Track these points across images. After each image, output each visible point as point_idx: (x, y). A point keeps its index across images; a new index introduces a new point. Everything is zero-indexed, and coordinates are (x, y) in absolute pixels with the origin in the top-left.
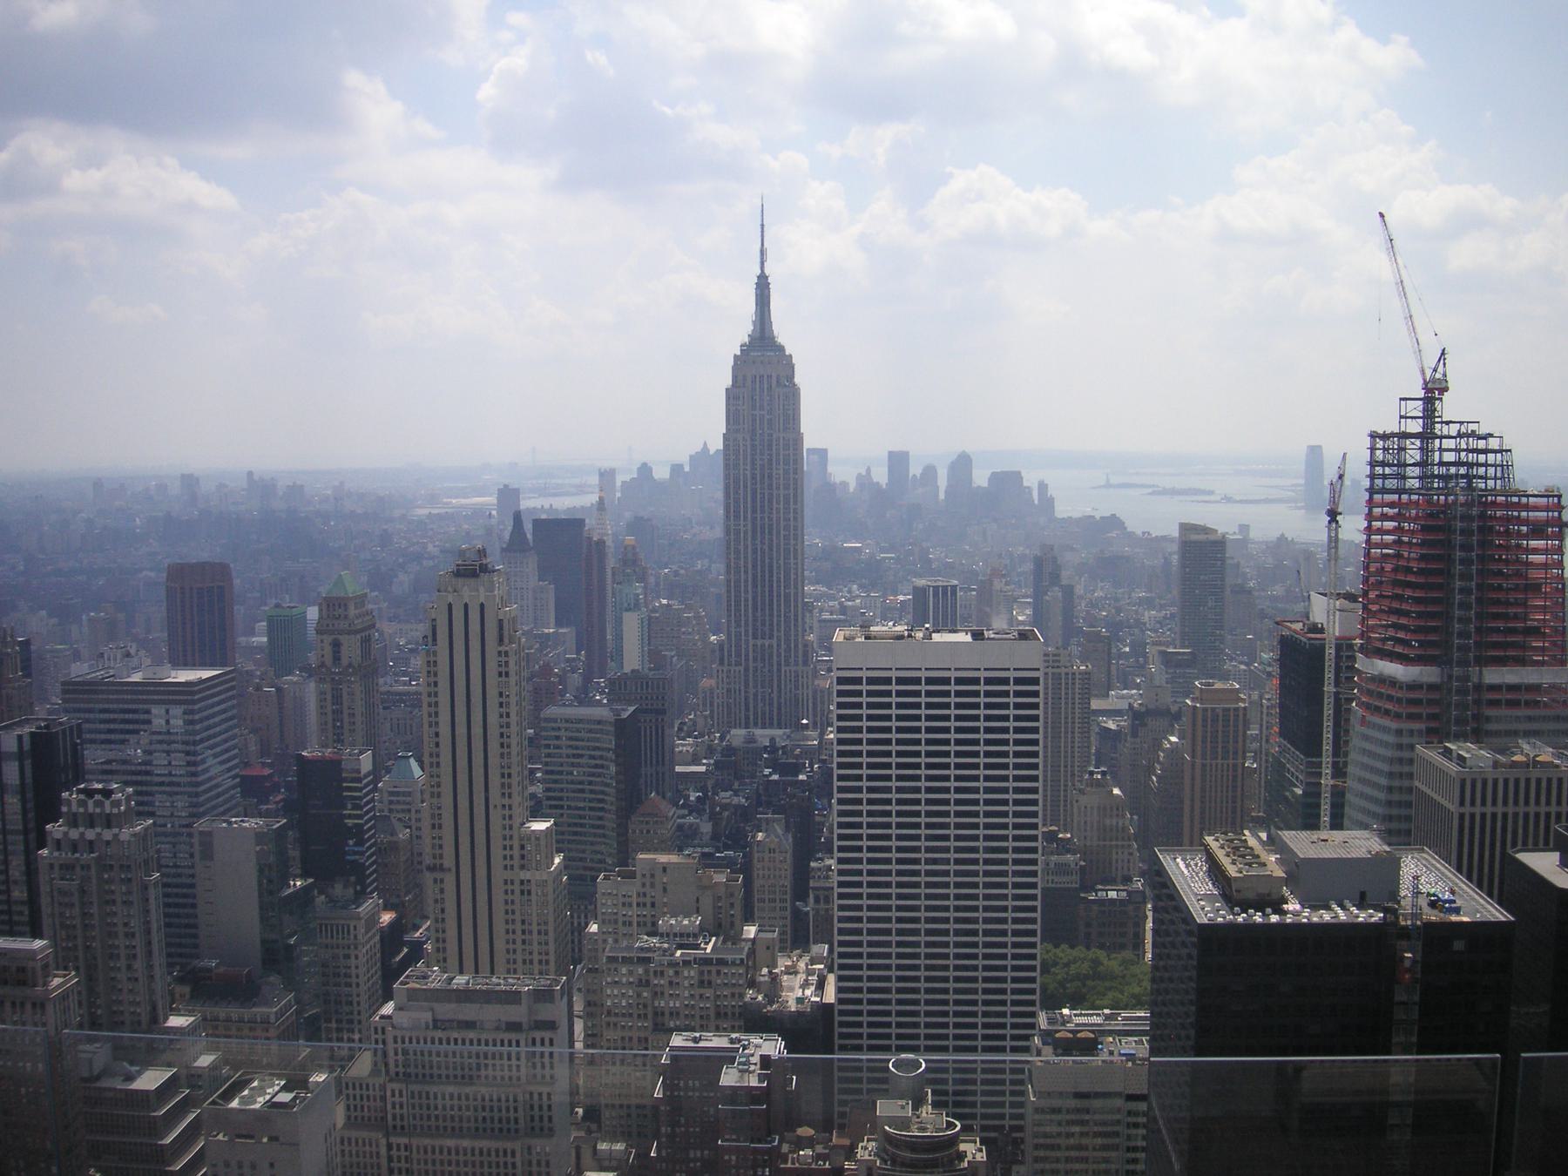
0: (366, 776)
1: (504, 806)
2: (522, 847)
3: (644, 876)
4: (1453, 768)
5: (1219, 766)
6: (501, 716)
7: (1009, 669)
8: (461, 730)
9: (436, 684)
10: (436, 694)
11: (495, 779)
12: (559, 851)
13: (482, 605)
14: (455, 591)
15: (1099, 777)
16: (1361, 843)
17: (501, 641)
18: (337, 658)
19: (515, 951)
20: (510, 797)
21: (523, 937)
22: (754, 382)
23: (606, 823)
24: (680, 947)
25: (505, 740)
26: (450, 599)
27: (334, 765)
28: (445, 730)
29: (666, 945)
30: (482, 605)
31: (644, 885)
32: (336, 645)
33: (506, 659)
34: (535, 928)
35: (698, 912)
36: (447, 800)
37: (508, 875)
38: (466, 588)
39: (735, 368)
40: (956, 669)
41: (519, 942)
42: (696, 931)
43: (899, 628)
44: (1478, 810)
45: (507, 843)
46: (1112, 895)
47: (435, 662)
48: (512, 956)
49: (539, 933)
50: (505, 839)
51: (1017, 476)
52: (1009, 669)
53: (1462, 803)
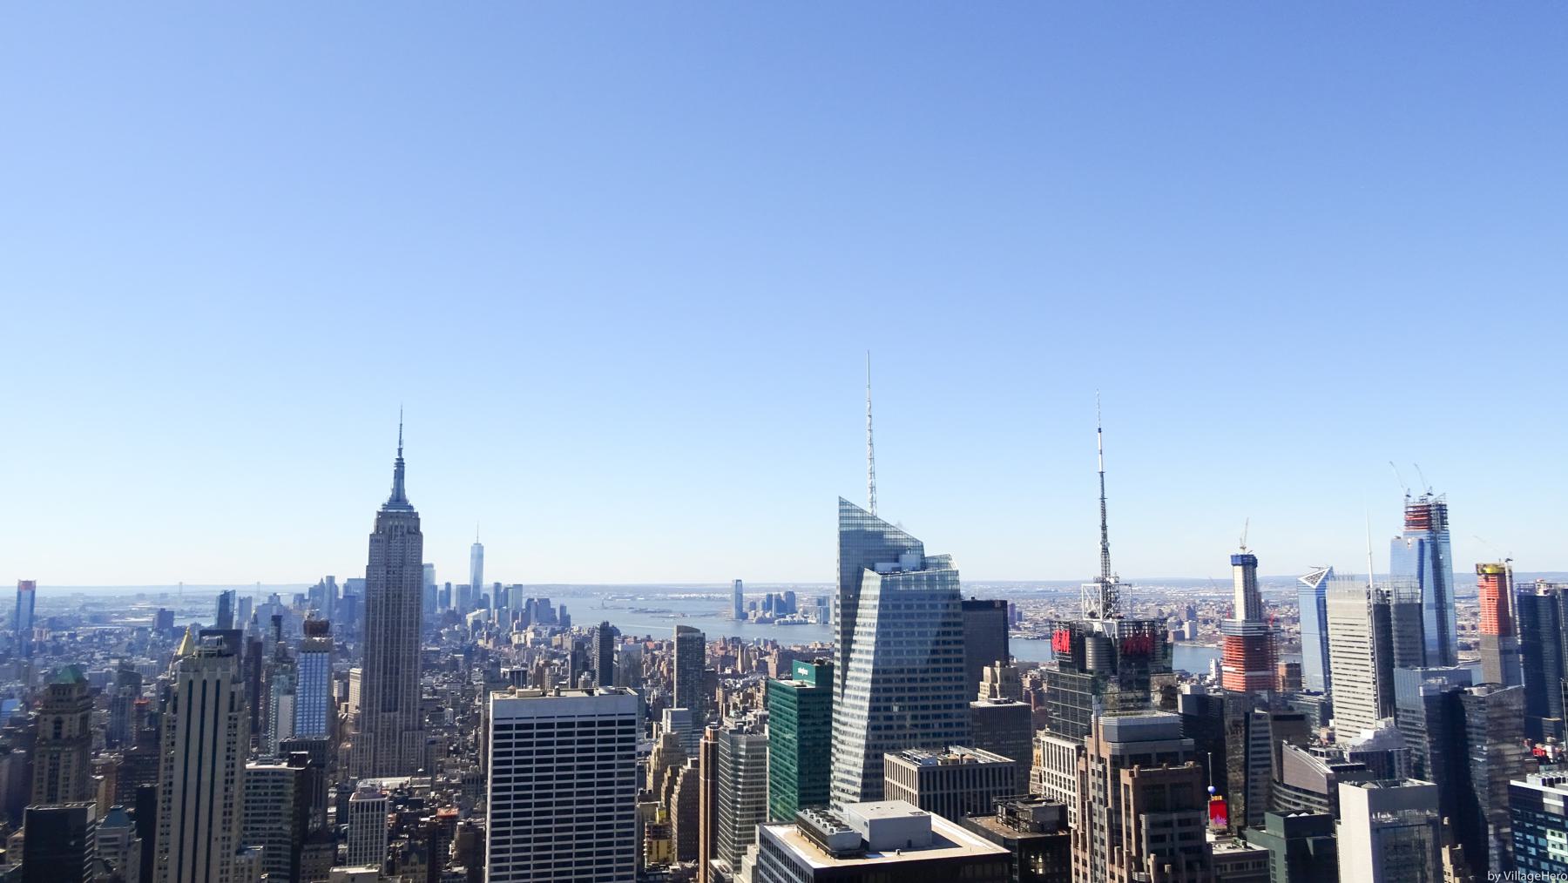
0: (94, 822)
1: (224, 838)
6: (227, 767)
7: (614, 715)
8: (192, 779)
12: (264, 871)
13: (218, 682)
14: (196, 671)
16: (900, 808)
17: (232, 709)
18: (57, 735)
20: (230, 830)
23: (283, 853)
26: (191, 677)
27: (63, 815)
30: (218, 682)
32: (58, 723)
38: (205, 668)
39: (378, 520)
40: (579, 716)
43: (536, 690)
44: (932, 793)
47: (174, 727)
51: (547, 601)
53: (921, 789)
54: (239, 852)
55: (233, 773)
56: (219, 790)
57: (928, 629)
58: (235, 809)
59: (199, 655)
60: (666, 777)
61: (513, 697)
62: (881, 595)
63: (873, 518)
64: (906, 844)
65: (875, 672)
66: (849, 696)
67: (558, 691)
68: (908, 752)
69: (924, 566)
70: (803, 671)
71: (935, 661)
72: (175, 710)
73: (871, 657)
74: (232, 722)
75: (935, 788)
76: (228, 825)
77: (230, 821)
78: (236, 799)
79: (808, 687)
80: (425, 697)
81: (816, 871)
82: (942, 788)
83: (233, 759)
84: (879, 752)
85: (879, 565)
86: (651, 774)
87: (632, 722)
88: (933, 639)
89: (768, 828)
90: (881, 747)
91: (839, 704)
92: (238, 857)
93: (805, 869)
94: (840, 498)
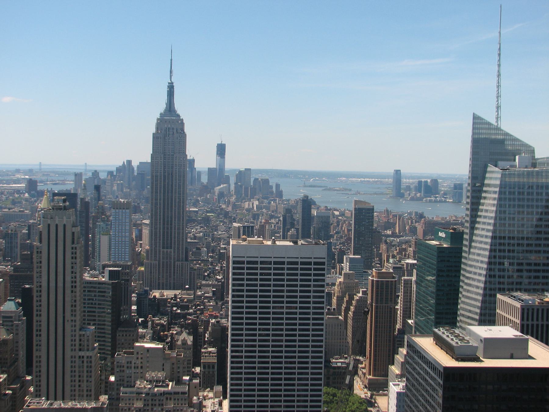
1: (72, 320)
2: (80, 340)
3: (138, 353)
4: (518, 305)
5: (384, 307)
6: (72, 278)
7: (311, 258)
8: (52, 284)
9: (41, 262)
10: (41, 267)
11: (68, 309)
12: (96, 341)
13: (65, 226)
14: (52, 218)
15: (332, 311)
19: (75, 390)
20: (75, 316)
21: (80, 383)
22: (166, 130)
24: (156, 386)
25: (74, 289)
28: (44, 284)
29: (149, 386)
30: (65, 226)
31: (138, 358)
33: (76, 251)
34: (85, 379)
35: (163, 370)
36: (44, 318)
37: (73, 354)
38: (57, 217)
41: (77, 386)
42: (164, 379)
43: (259, 239)
44: (530, 323)
45: (73, 338)
46: (339, 364)
47: (41, 252)
48: (73, 393)
49: (87, 381)
50: (72, 336)
52: (311, 258)
53: (522, 319)
54: (80, 330)
55: (75, 282)
56: (68, 292)
57: (535, 210)
58: (78, 303)
59: (53, 209)
60: (345, 299)
61: (244, 243)
62: (501, 184)
63: (498, 129)
64: (509, 355)
65: (493, 238)
66: (474, 254)
67: (274, 242)
68: (515, 294)
69: (534, 165)
70: (442, 235)
71: (538, 232)
72: (41, 242)
73: (491, 228)
74: (74, 251)
75: (532, 320)
76: (74, 313)
77: (75, 311)
78: (78, 298)
79: (445, 246)
80: (189, 240)
81: (446, 369)
82: (537, 320)
83: (75, 273)
84: (493, 292)
85: (500, 163)
86: (335, 298)
87: (323, 264)
88: (538, 217)
89: (413, 338)
90: (494, 289)
91: (466, 258)
92: (81, 333)
93: (437, 366)
94: (474, 114)
